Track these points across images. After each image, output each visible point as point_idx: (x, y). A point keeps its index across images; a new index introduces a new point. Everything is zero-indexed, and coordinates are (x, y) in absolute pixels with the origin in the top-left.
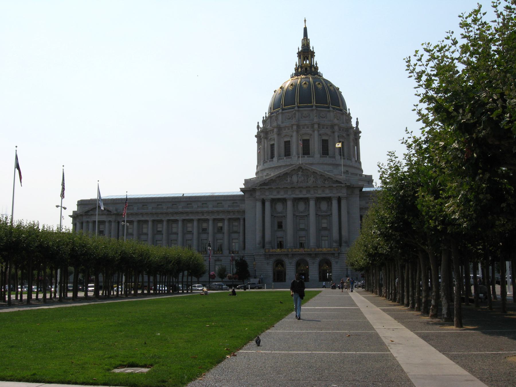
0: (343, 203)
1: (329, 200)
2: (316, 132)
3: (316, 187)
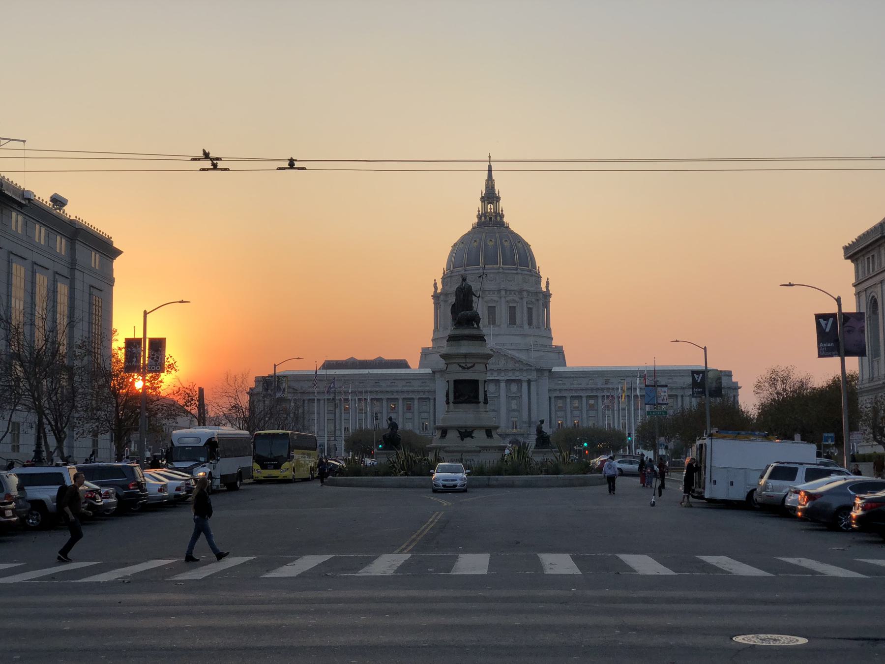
0: (533, 386)
1: (519, 381)
2: (503, 299)
3: (506, 370)
